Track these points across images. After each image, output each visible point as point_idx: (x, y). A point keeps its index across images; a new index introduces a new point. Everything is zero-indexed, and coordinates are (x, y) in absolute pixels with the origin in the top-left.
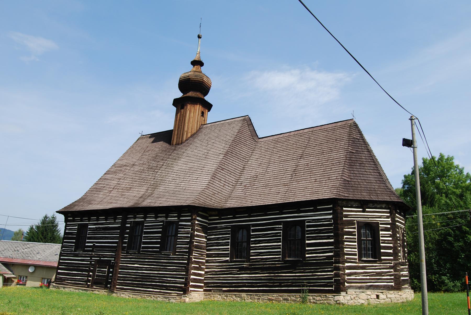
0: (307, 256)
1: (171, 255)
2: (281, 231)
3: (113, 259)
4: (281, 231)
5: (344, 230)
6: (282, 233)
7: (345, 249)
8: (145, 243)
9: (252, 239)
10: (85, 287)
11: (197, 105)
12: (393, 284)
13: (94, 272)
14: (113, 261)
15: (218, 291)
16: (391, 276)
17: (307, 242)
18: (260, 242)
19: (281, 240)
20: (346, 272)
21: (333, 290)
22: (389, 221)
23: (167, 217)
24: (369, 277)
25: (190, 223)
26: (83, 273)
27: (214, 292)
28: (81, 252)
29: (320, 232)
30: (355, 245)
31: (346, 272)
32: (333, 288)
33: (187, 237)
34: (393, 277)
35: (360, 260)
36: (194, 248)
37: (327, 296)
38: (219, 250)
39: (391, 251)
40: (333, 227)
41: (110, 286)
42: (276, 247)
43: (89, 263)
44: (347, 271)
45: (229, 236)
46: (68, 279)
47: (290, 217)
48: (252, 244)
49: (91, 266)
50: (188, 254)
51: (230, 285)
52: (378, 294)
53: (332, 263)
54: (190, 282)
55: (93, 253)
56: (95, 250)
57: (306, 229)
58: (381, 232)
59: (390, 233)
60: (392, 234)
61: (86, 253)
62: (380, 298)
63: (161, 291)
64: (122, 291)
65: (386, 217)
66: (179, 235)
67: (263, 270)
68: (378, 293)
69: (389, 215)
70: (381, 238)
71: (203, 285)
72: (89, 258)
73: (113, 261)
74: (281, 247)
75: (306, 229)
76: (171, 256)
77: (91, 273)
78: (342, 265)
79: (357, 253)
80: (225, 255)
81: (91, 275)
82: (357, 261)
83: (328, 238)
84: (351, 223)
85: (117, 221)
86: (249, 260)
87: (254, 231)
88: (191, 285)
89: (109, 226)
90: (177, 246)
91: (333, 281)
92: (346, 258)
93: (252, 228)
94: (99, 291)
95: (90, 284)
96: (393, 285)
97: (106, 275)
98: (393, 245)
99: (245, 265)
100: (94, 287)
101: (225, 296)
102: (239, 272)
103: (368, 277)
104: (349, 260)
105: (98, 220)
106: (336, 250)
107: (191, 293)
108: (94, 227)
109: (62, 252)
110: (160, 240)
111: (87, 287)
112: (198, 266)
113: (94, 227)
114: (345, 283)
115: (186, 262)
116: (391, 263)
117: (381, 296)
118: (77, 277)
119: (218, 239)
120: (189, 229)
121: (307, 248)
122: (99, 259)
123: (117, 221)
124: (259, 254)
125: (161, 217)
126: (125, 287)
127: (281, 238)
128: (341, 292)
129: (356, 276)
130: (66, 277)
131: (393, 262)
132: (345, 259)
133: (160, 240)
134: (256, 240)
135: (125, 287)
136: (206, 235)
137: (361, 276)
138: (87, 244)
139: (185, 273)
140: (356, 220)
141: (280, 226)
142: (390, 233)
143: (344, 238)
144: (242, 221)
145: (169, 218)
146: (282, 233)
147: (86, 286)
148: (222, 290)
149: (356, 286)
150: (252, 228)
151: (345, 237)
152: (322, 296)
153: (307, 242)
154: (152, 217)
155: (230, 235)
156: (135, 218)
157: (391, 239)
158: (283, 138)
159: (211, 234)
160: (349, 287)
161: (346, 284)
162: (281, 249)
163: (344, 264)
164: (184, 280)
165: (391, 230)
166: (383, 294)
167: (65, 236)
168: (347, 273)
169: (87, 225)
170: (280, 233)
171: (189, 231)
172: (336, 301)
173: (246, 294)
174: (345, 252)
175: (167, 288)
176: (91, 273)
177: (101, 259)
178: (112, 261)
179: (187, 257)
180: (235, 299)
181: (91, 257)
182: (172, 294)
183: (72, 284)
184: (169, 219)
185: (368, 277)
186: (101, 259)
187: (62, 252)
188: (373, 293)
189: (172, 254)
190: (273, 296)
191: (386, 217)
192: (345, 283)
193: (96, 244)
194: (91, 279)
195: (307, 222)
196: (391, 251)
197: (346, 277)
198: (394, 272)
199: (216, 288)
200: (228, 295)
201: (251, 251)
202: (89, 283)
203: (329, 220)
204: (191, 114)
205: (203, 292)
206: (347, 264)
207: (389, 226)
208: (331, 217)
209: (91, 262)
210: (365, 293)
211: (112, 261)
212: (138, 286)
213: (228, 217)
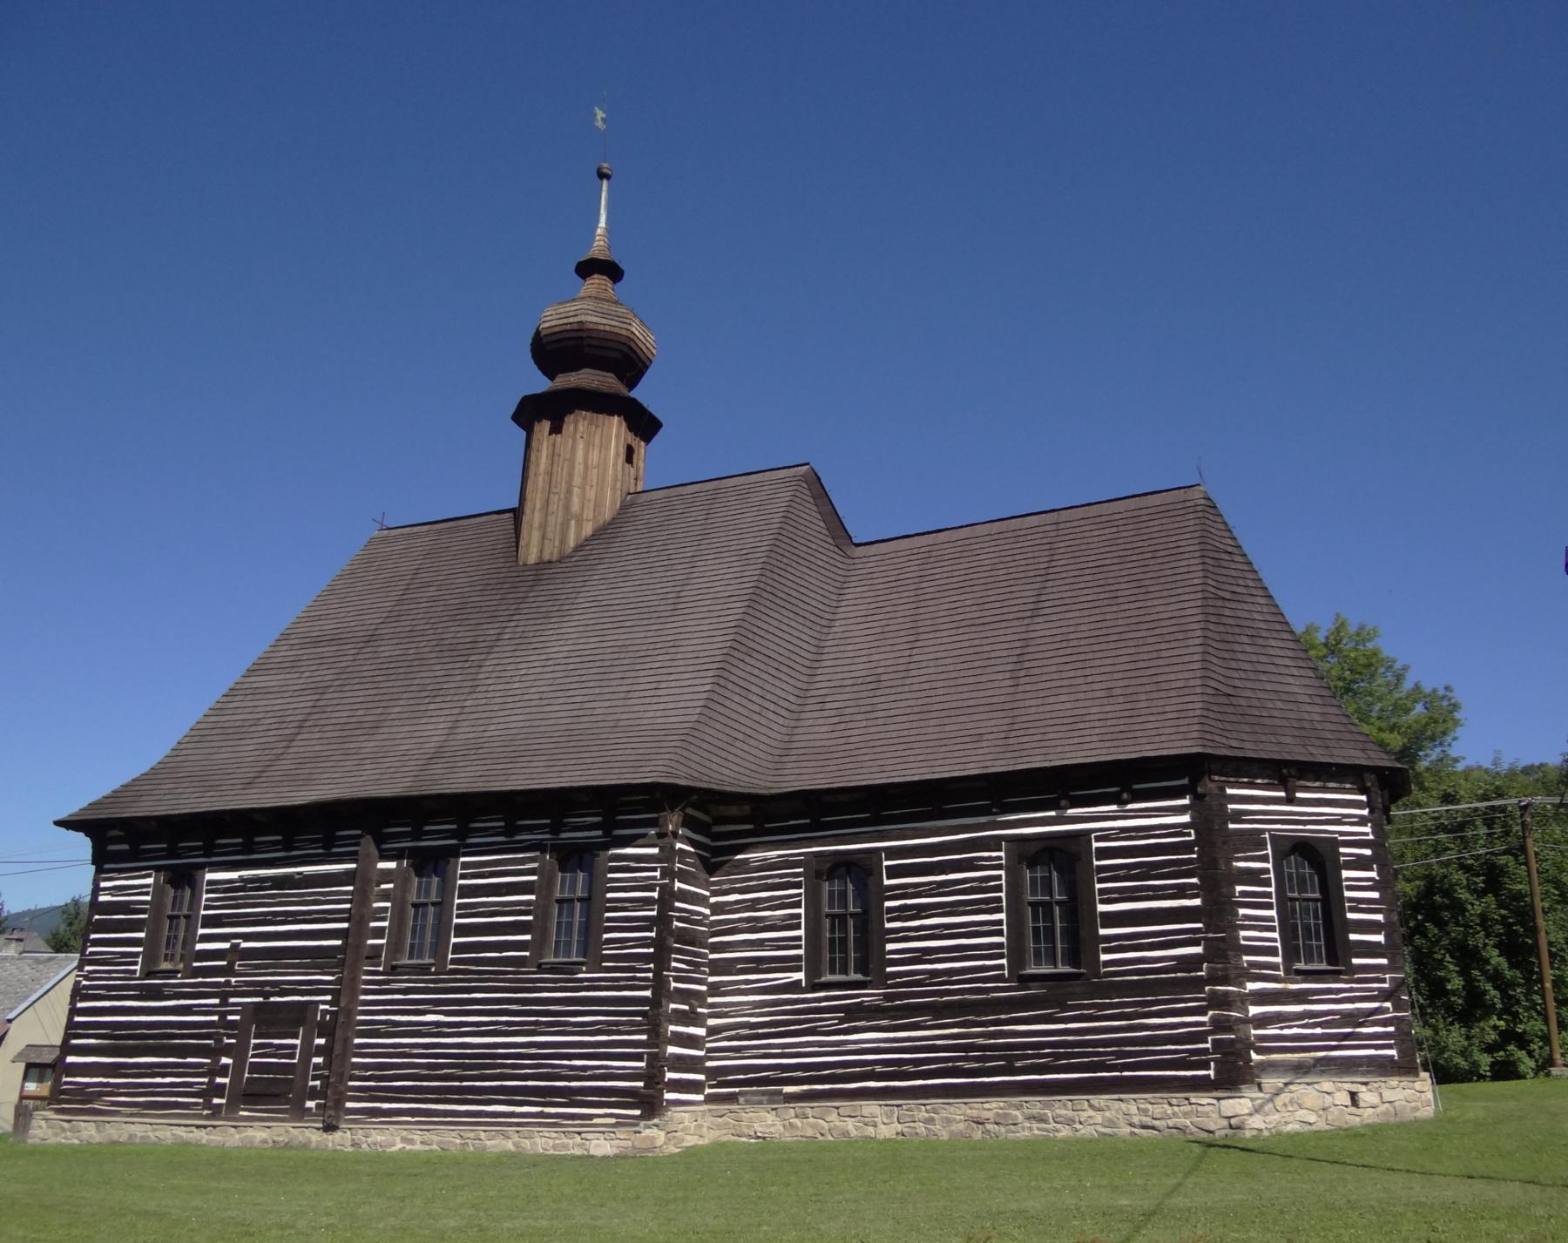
0: (1104, 957)
3: (329, 998)
4: (1002, 873)
5: (1234, 864)
6: (1004, 878)
7: (1243, 933)
8: (462, 930)
9: (888, 904)
10: (200, 1117)
11: (613, 415)
12: (1393, 1052)
14: (327, 1007)
15: (765, 1098)
16: (1385, 1026)
17: (1101, 908)
18: (921, 911)
19: (1004, 904)
20: (1250, 1015)
21: (1212, 1077)
22: (1367, 834)
23: (556, 829)
24: (1322, 1028)
26: (190, 1060)
27: (748, 1102)
29: (1148, 871)
30: (1271, 919)
31: (1250, 1015)
32: (1211, 1073)
33: (647, 902)
34: (1391, 1029)
35: (1293, 974)
36: (676, 943)
37: (1193, 1100)
38: (760, 944)
39: (1380, 938)
40: (1195, 856)
41: (317, 1104)
42: (986, 928)
43: (215, 1018)
44: (1254, 1010)
45: (800, 895)
46: (115, 1090)
48: (890, 920)
49: (222, 1031)
50: (652, 965)
51: (813, 1073)
52: (1354, 1088)
53: (1198, 984)
54: (666, 1068)
55: (233, 980)
56: (239, 965)
57: (1096, 863)
58: (1345, 874)
59: (1373, 874)
60: (1377, 878)
61: (200, 980)
62: (1362, 1104)
64: (374, 1120)
65: (1356, 820)
67: (939, 1011)
68: (1355, 1085)
69: (1365, 812)
70: (1347, 894)
71: (702, 1077)
72: (216, 1001)
73: (327, 1007)
74: (1005, 927)
75: (1096, 863)
77: (225, 1060)
78: (1235, 989)
79: (1278, 944)
80: (789, 964)
81: (226, 1066)
82: (1282, 973)
83: (1181, 892)
84: (1253, 841)
86: (883, 980)
87: (894, 872)
88: (669, 1079)
90: (605, 936)
92: (1245, 965)
93: (886, 863)
94: (269, 1127)
95: (223, 1101)
96: (1394, 1056)
97: (296, 1061)
98: (1384, 918)
99: (870, 996)
100: (241, 1113)
102: (846, 1025)
103: (1318, 1031)
104: (1257, 971)
105: (249, 848)
106: (1211, 935)
107: (670, 1110)
109: (84, 983)
111: (207, 1117)
112: (687, 1008)
113: (234, 875)
114: (1252, 1052)
115: (648, 993)
116: (1383, 981)
117: (1366, 1096)
118: (159, 1080)
119: (754, 905)
120: (654, 869)
121: (1102, 932)
122: (261, 999)
124: (923, 955)
125: (530, 829)
126: (386, 1106)
127: (1000, 897)
128: (1241, 1086)
129: (1281, 1028)
130: (105, 1080)
131: (1387, 976)
132: (1244, 968)
134: (906, 904)
135: (386, 1106)
136: (707, 894)
137: (1298, 1026)
139: (644, 1037)
140: (1269, 830)
141: (994, 854)
142: (1373, 874)
143: (1237, 895)
145: (565, 831)
146: (1004, 878)
147: (205, 1112)
148: (780, 1092)
149: (1278, 1061)
150: (886, 863)
151: (1239, 888)
152: (1174, 1101)
153: (1101, 908)
155: (802, 891)
156: (418, 835)
157: (1375, 895)
158: (951, 545)
159: (725, 887)
160: (1266, 1067)
161: (1254, 1056)
162: (1003, 936)
163: (1242, 985)
165: (1375, 866)
166: (1369, 1087)
167: (97, 917)
168: (1254, 1015)
170: (999, 878)
171: (654, 878)
172: (1229, 1118)
173: (881, 1105)
174: (1243, 942)
175: (572, 1098)
176: (225, 1060)
177: (272, 999)
178: (322, 1007)
179: (651, 975)
180: (837, 1123)
181: (224, 997)
182: (596, 1121)
183: (135, 1110)
184: (564, 835)
185: (1318, 1031)
186: (272, 999)
187: (84, 983)
188: (1340, 1085)
189: (584, 969)
190: (987, 1106)
191: (1356, 820)
192: (1252, 1052)
194: (226, 1080)
195: (1098, 839)
196: (1380, 938)
197: (1253, 1032)
198: (1396, 1009)
199: (755, 1088)
200: (809, 1111)
201: (889, 947)
202: (216, 1101)
203: (1178, 829)
204: (591, 453)
205: (705, 1107)
206: (1252, 986)
207: (1368, 852)
208: (1186, 818)
209: (223, 1015)
210: (1316, 1086)
211: (322, 1007)
212: (443, 1095)
213: (792, 822)
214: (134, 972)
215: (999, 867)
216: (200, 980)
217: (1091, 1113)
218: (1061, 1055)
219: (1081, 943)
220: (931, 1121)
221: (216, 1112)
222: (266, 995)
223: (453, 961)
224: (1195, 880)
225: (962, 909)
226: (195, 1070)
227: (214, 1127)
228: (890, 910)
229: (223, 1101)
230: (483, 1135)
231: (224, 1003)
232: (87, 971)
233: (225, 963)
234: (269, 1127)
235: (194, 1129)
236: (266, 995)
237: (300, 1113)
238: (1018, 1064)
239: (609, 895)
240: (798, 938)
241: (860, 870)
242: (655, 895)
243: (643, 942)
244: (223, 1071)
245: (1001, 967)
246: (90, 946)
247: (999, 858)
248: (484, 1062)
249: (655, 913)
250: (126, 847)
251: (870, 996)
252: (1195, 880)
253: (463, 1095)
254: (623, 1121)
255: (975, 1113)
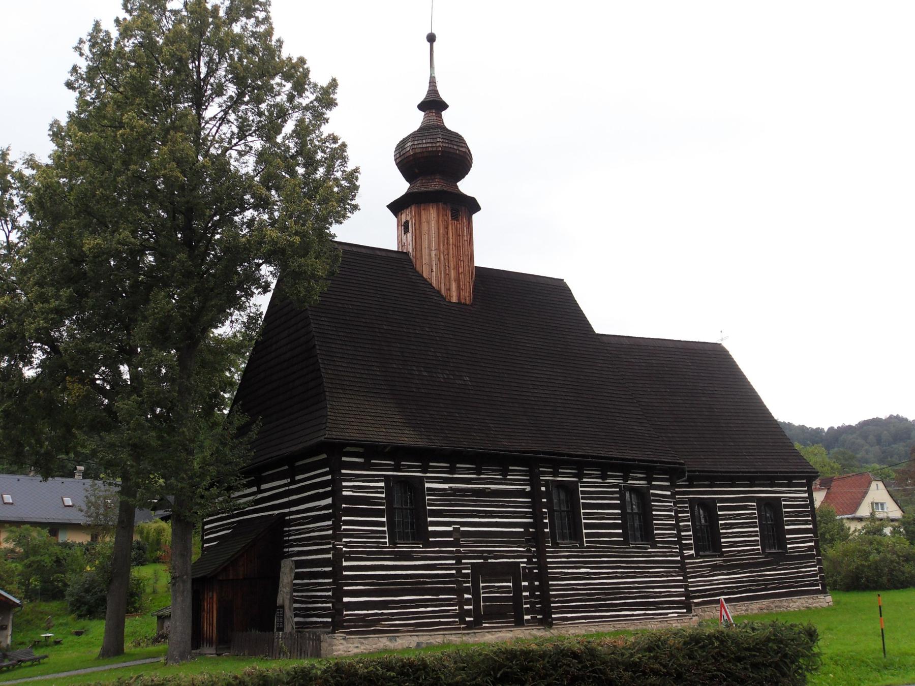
0: (789, 546)
1: (648, 548)
2: (756, 511)
3: (525, 560)
4: (756, 511)
8: (588, 526)
9: (720, 522)
10: (459, 629)
13: (476, 592)
14: (525, 565)
18: (732, 526)
23: (626, 479)
25: (669, 493)
26: (441, 597)
28: (420, 548)
32: (820, 587)
33: (670, 516)
43: (454, 572)
46: (391, 617)
47: (765, 492)
48: (722, 529)
49: (460, 579)
53: (813, 556)
55: (461, 549)
61: (437, 549)
63: (647, 612)
66: (654, 513)
67: (743, 567)
72: (454, 562)
73: (525, 565)
75: (784, 510)
76: (649, 550)
77: (466, 596)
83: (806, 522)
85: (508, 477)
86: (722, 554)
89: (490, 488)
90: (655, 532)
91: (818, 578)
93: (718, 505)
94: (511, 631)
97: (512, 595)
99: (719, 561)
100: (484, 625)
101: (702, 612)
105: (452, 470)
108: (446, 486)
109: (344, 549)
110: (620, 522)
111: (464, 629)
113: (446, 486)
120: (670, 502)
121: (787, 536)
122: (482, 561)
123: (508, 477)
124: (734, 544)
125: (612, 477)
133: (620, 522)
138: (430, 529)
139: (682, 578)
141: (753, 504)
144: (704, 493)
147: (462, 626)
154: (593, 476)
156: (555, 474)
164: (683, 590)
167: (344, 506)
169: (421, 480)
170: (755, 514)
171: (671, 506)
176: (466, 596)
177: (489, 561)
178: (522, 565)
179: (678, 550)
182: (669, 615)
184: (629, 482)
186: (489, 561)
187: (344, 549)
193: (462, 529)
195: (784, 501)
200: (706, 609)
201: (723, 540)
202: (467, 619)
211: (522, 565)
212: (597, 608)
214: (385, 543)
215: (754, 509)
216: (437, 549)
217: (792, 604)
218: (780, 583)
219: (781, 542)
220: (747, 610)
221: (470, 626)
222: (486, 558)
223: (587, 542)
224: (810, 518)
225: (745, 525)
226: (448, 602)
227: (474, 633)
228: (722, 525)
229: (472, 619)
230: (625, 626)
231: (459, 562)
232: (344, 542)
233: (452, 539)
234: (511, 631)
235: (460, 635)
236: (486, 558)
237: (519, 622)
238: (769, 587)
239: (654, 513)
240: (690, 536)
241: (709, 507)
242: (673, 514)
243: (671, 535)
244: (468, 602)
245: (759, 549)
246: (343, 525)
247: (754, 506)
248: (615, 591)
249: (674, 522)
250: (361, 460)
251: (719, 561)
252: (810, 518)
253: (608, 607)
254: (681, 615)
255: (760, 606)
